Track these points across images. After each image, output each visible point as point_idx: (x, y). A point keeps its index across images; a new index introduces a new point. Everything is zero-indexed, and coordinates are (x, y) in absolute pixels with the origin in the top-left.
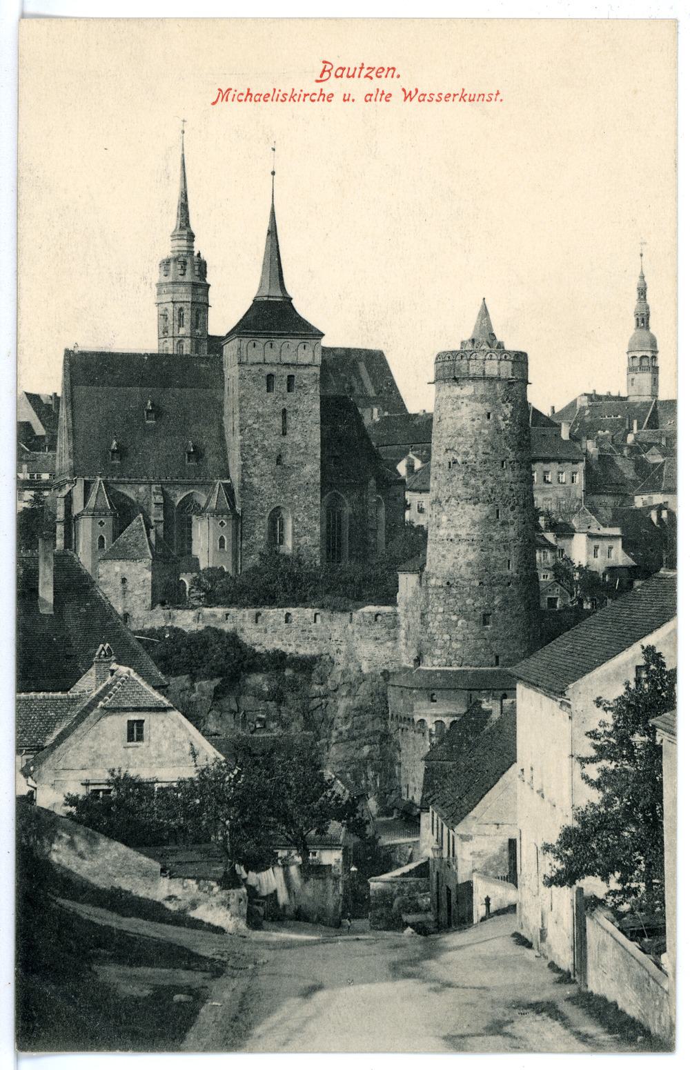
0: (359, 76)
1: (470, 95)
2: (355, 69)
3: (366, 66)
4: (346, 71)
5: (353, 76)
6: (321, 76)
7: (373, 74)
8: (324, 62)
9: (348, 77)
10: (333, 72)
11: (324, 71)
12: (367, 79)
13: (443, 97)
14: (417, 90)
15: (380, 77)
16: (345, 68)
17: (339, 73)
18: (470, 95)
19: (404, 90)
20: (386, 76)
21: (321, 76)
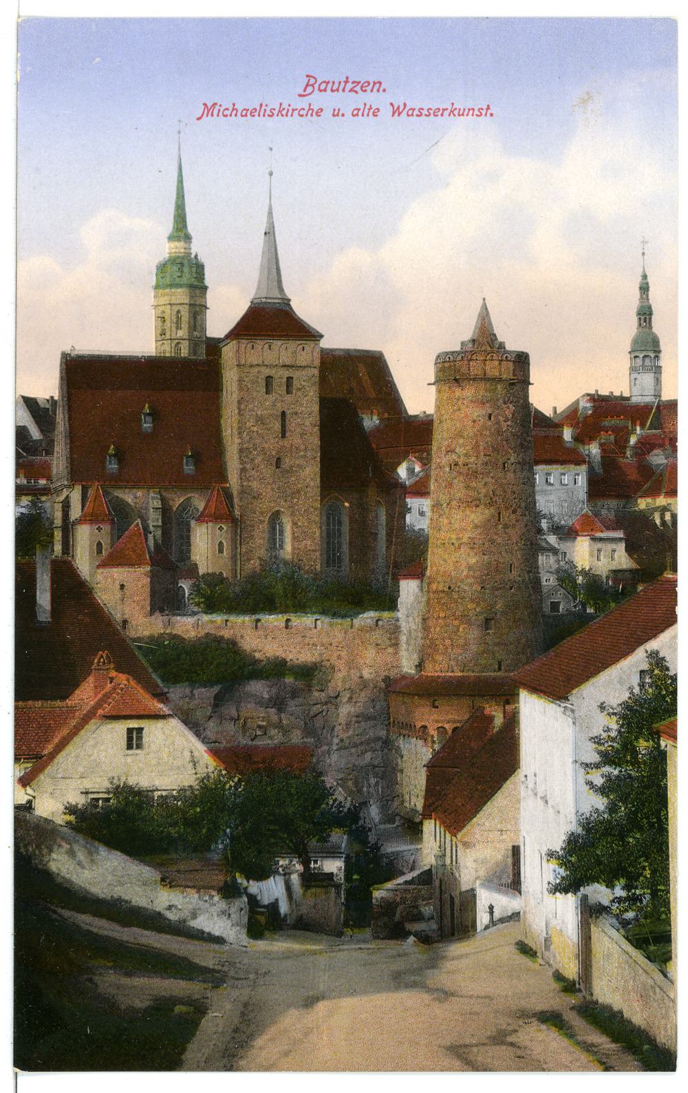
1: (460, 109)
2: (340, 83)
4: (330, 86)
16: (328, 83)
17: (323, 87)
18: (460, 109)
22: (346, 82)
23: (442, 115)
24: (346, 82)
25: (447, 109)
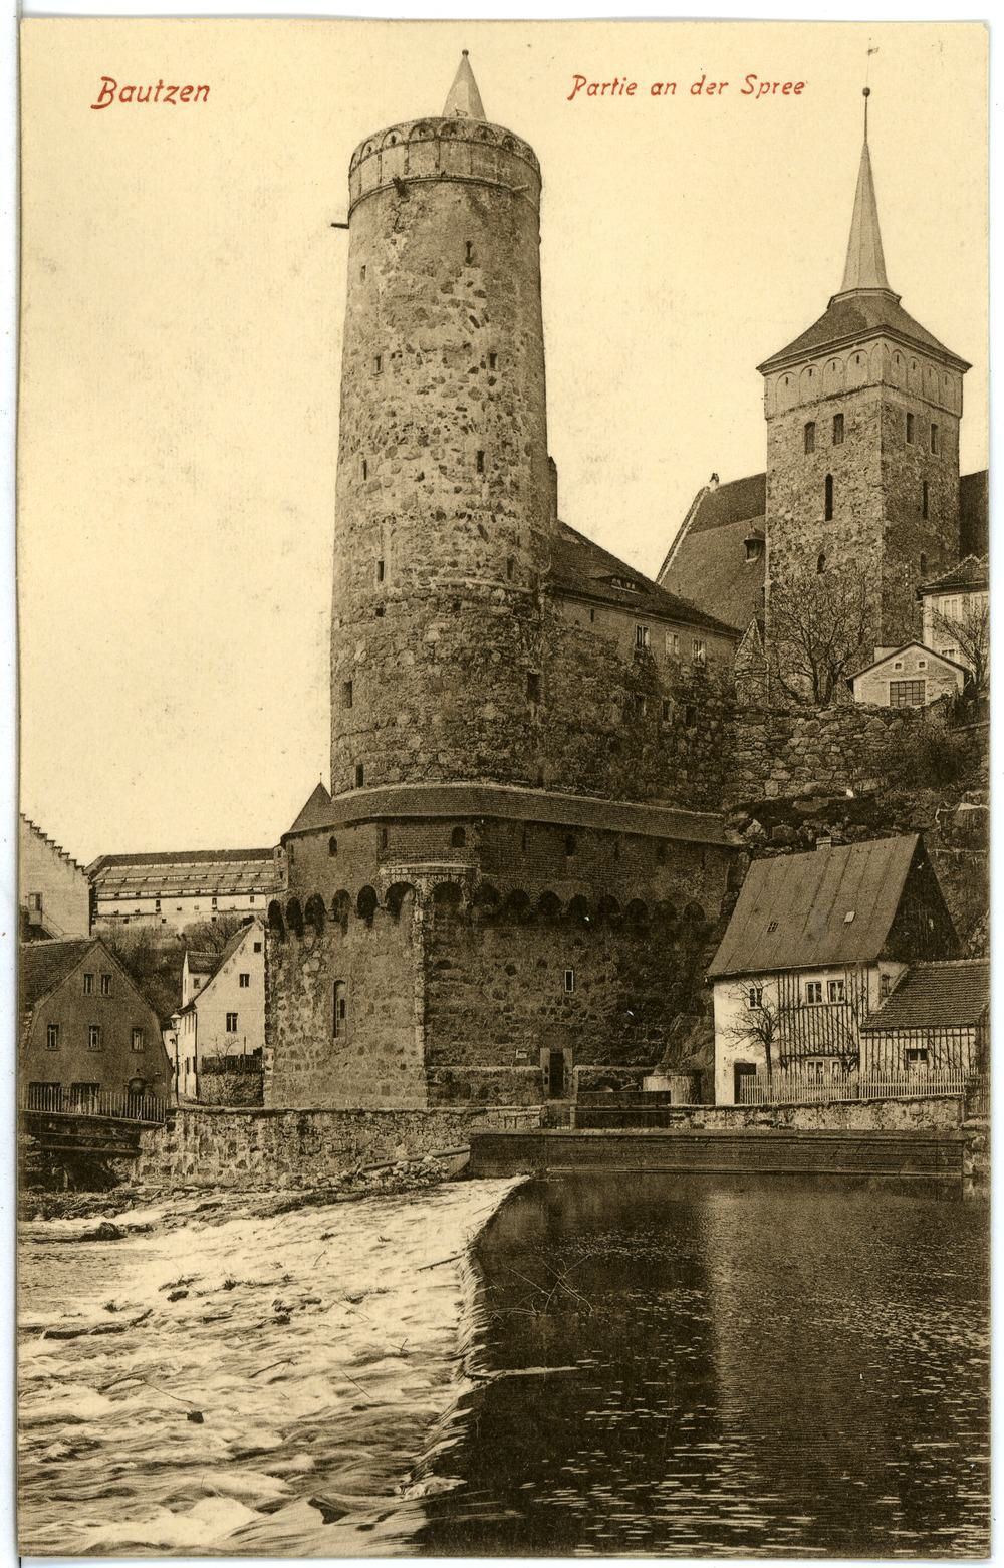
0: (156, 100)
2: (150, 89)
3: (166, 84)
4: (136, 93)
5: (146, 99)
6: (100, 100)
8: (104, 79)
9: (139, 100)
10: (117, 93)
11: (105, 91)
15: (187, 100)
17: (126, 95)
20: (196, 99)
21: (100, 100)
22: (160, 88)
24: (160, 88)
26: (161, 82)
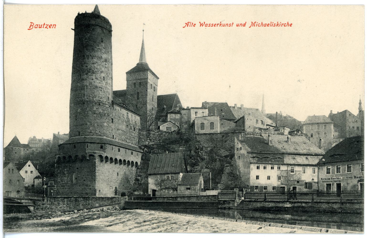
0: (43, 27)
2: (42, 25)
4: (39, 25)
7: (48, 27)
9: (39, 28)
12: (46, 28)
13: (213, 25)
14: (204, 23)
16: (38, 25)
19: (200, 22)
23: (217, 26)
24: (44, 24)
25: (219, 24)
26: (44, 23)
